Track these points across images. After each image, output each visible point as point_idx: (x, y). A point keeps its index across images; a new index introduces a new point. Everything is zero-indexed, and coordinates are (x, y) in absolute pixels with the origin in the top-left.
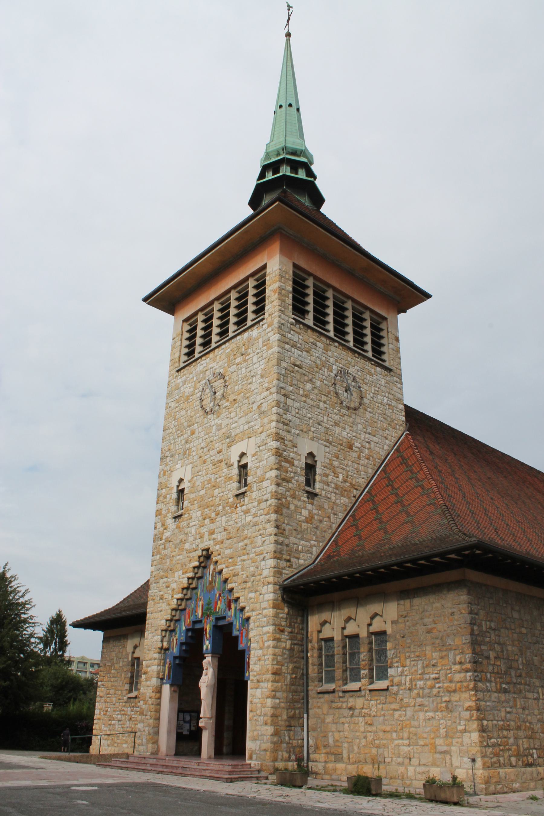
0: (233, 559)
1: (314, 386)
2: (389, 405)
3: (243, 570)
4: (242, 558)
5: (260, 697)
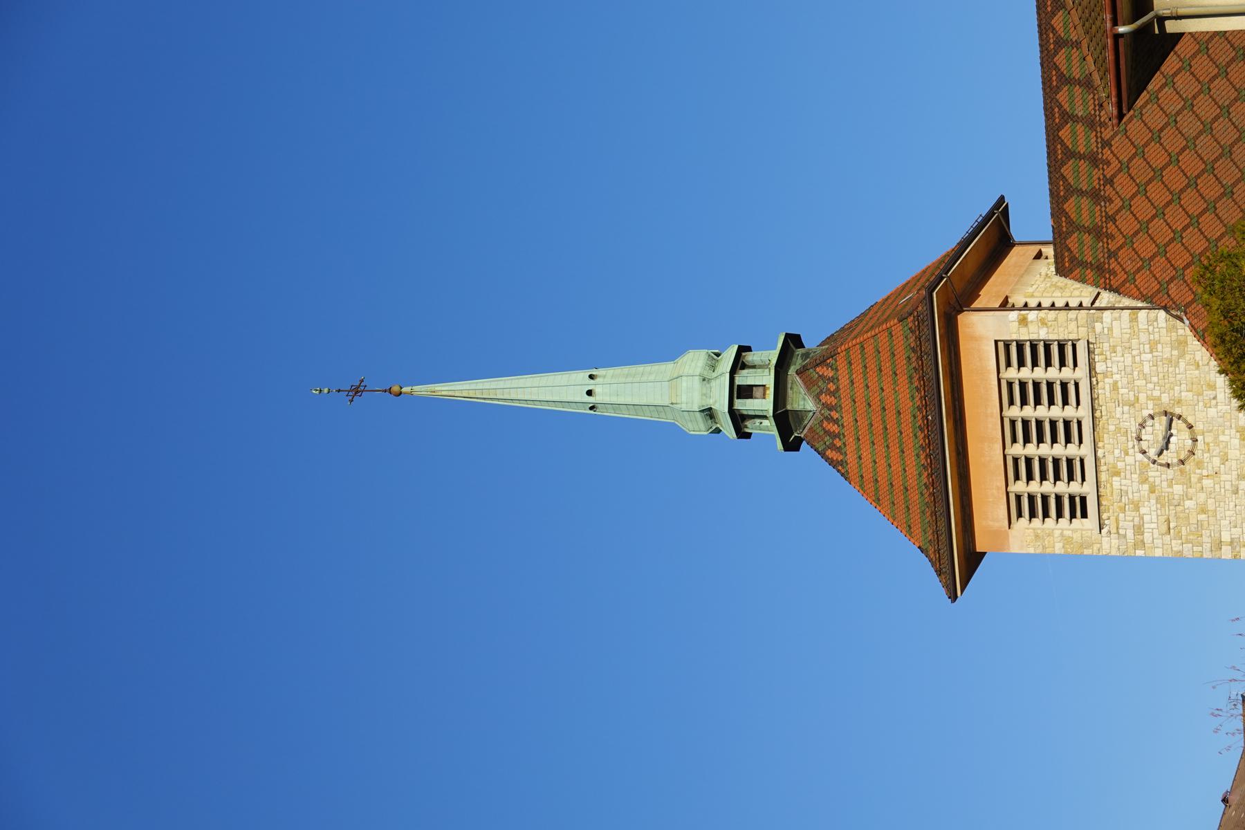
1: (1185, 498)
2: (1151, 352)
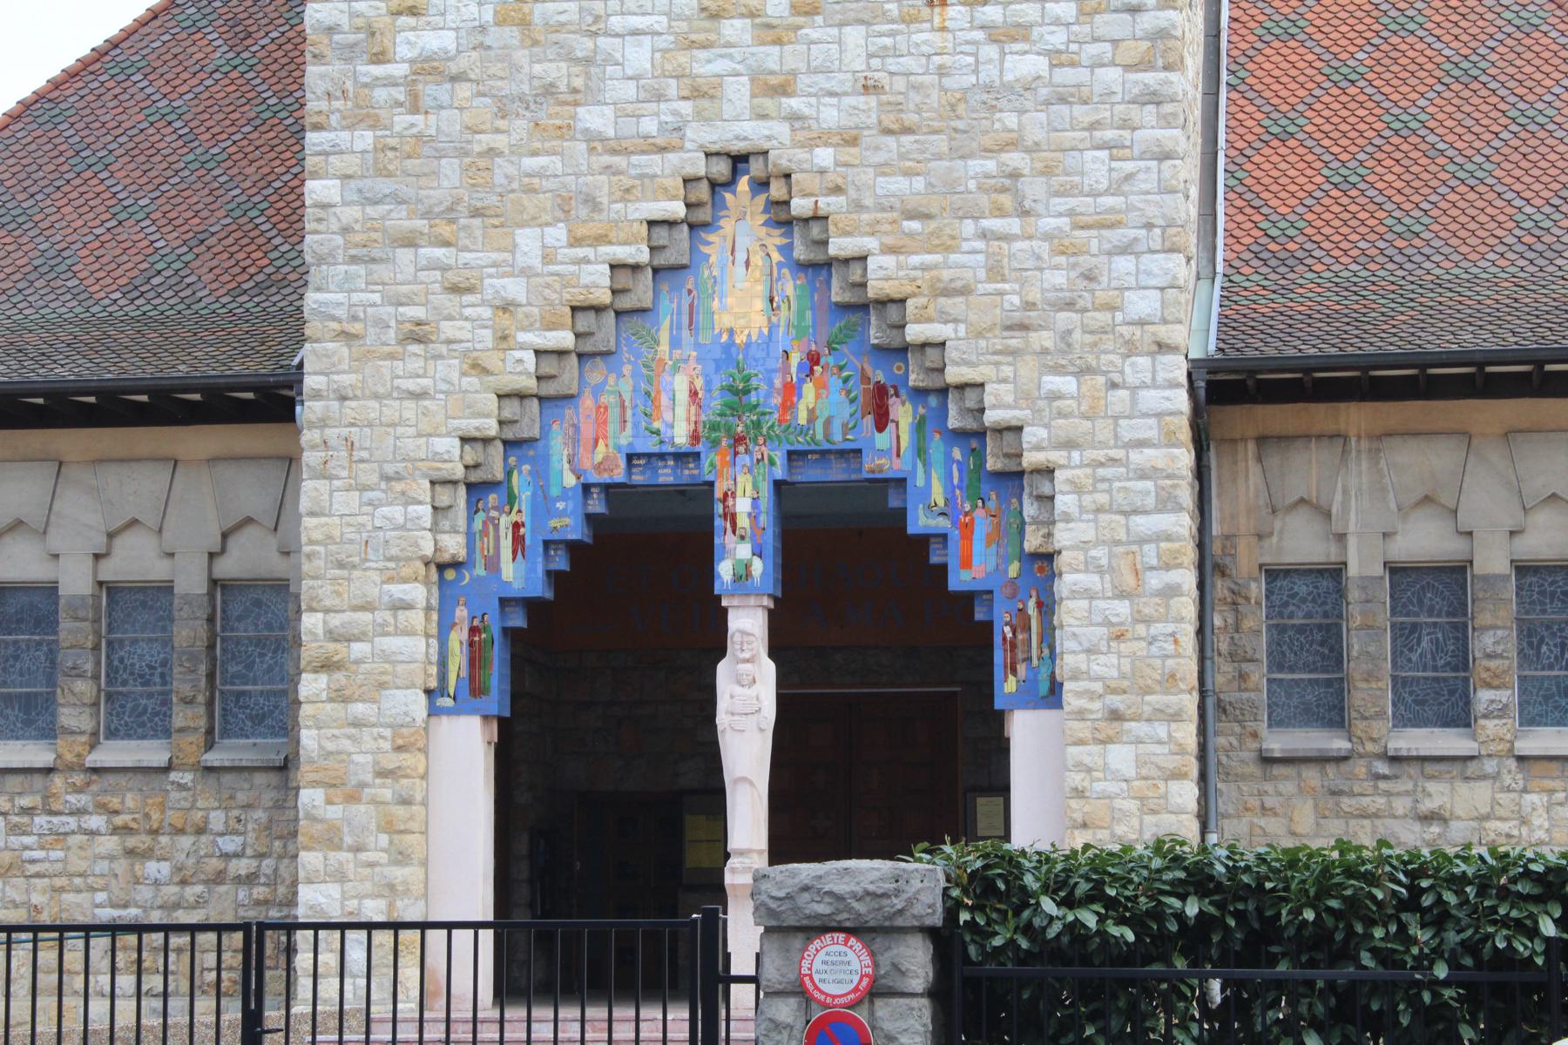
0: (933, 225)
3: (995, 272)
4: (987, 223)
5: (1131, 772)
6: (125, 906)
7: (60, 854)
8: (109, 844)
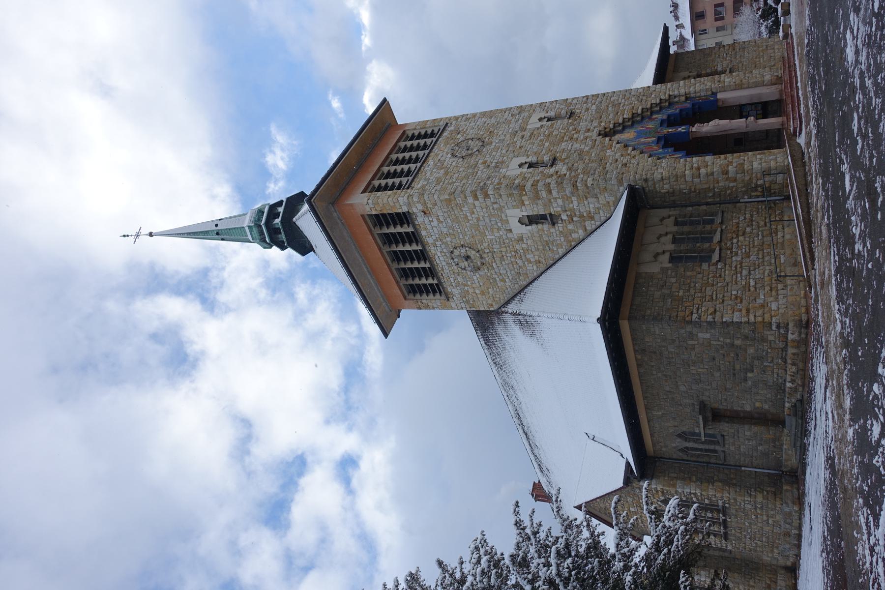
6: (759, 235)
7: (744, 247)
8: (741, 238)
